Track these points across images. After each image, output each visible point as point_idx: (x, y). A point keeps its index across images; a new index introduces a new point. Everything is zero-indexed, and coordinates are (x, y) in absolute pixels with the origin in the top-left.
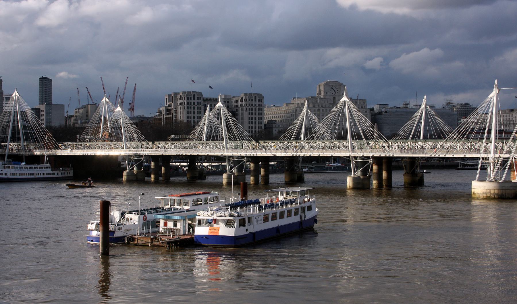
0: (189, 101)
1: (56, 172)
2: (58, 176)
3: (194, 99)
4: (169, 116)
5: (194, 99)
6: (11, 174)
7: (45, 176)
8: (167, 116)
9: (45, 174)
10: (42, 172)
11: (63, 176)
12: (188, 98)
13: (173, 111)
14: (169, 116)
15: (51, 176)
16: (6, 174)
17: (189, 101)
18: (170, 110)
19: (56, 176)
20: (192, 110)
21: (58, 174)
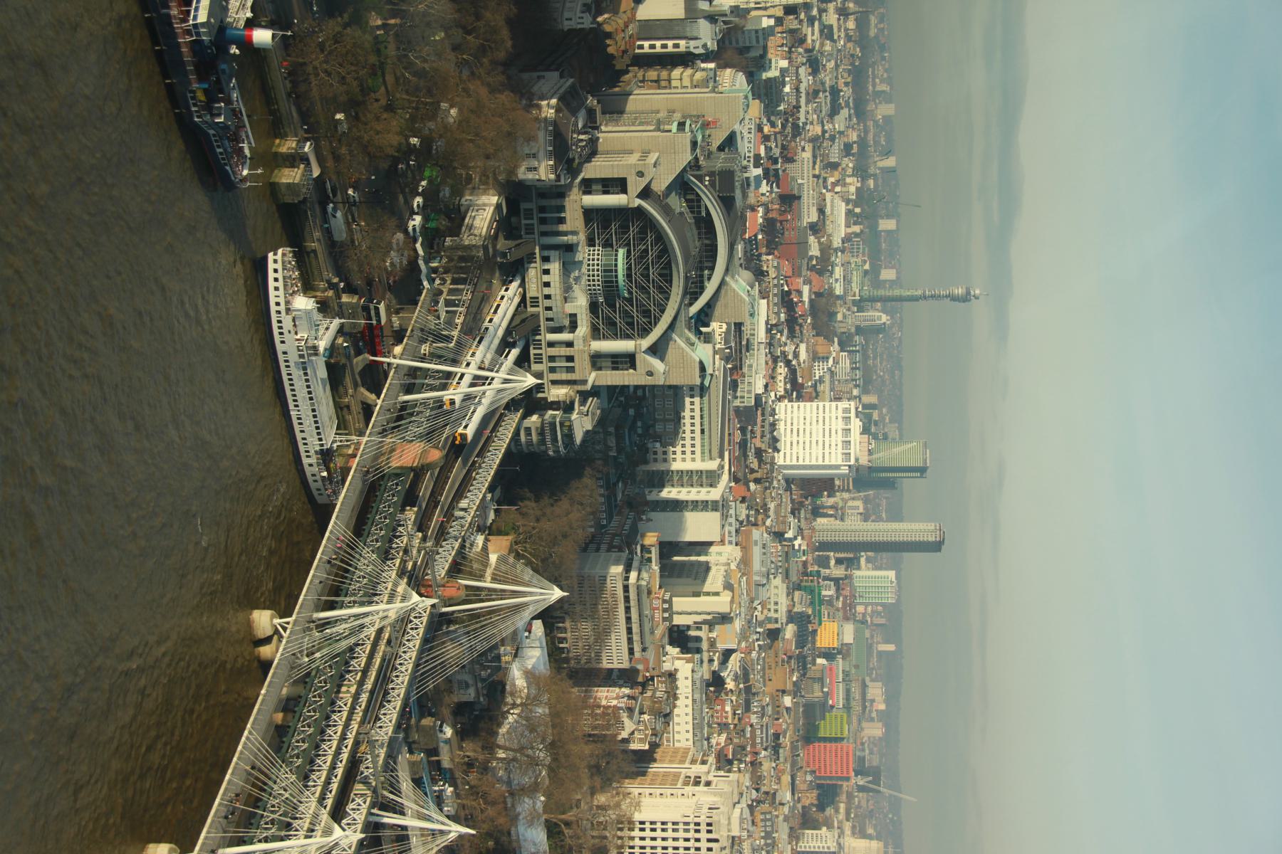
0: (703, 827)
1: (313, 460)
2: (306, 466)
3: (709, 840)
4: (681, 781)
5: (709, 840)
6: (285, 353)
7: (299, 436)
8: (682, 776)
9: (303, 435)
10: (305, 427)
11: (310, 479)
12: (709, 824)
13: (690, 789)
14: (681, 781)
15: (302, 448)
16: (283, 342)
17: (703, 827)
18: (697, 783)
19: (306, 461)
20: (681, 834)
21: (311, 465)
